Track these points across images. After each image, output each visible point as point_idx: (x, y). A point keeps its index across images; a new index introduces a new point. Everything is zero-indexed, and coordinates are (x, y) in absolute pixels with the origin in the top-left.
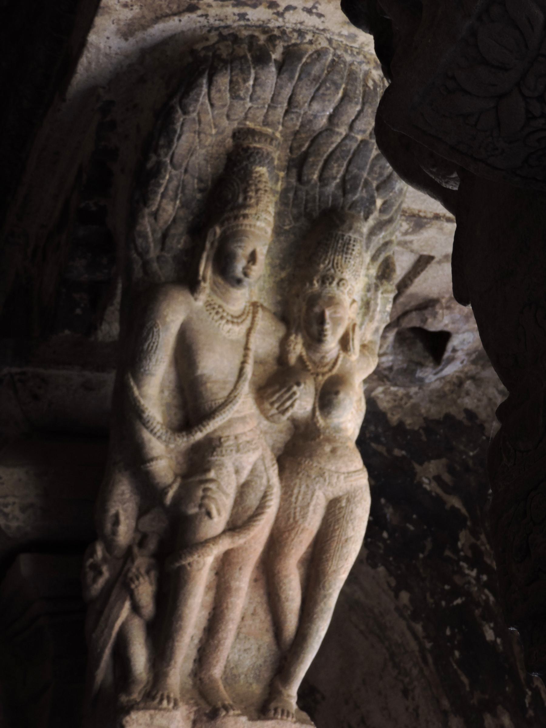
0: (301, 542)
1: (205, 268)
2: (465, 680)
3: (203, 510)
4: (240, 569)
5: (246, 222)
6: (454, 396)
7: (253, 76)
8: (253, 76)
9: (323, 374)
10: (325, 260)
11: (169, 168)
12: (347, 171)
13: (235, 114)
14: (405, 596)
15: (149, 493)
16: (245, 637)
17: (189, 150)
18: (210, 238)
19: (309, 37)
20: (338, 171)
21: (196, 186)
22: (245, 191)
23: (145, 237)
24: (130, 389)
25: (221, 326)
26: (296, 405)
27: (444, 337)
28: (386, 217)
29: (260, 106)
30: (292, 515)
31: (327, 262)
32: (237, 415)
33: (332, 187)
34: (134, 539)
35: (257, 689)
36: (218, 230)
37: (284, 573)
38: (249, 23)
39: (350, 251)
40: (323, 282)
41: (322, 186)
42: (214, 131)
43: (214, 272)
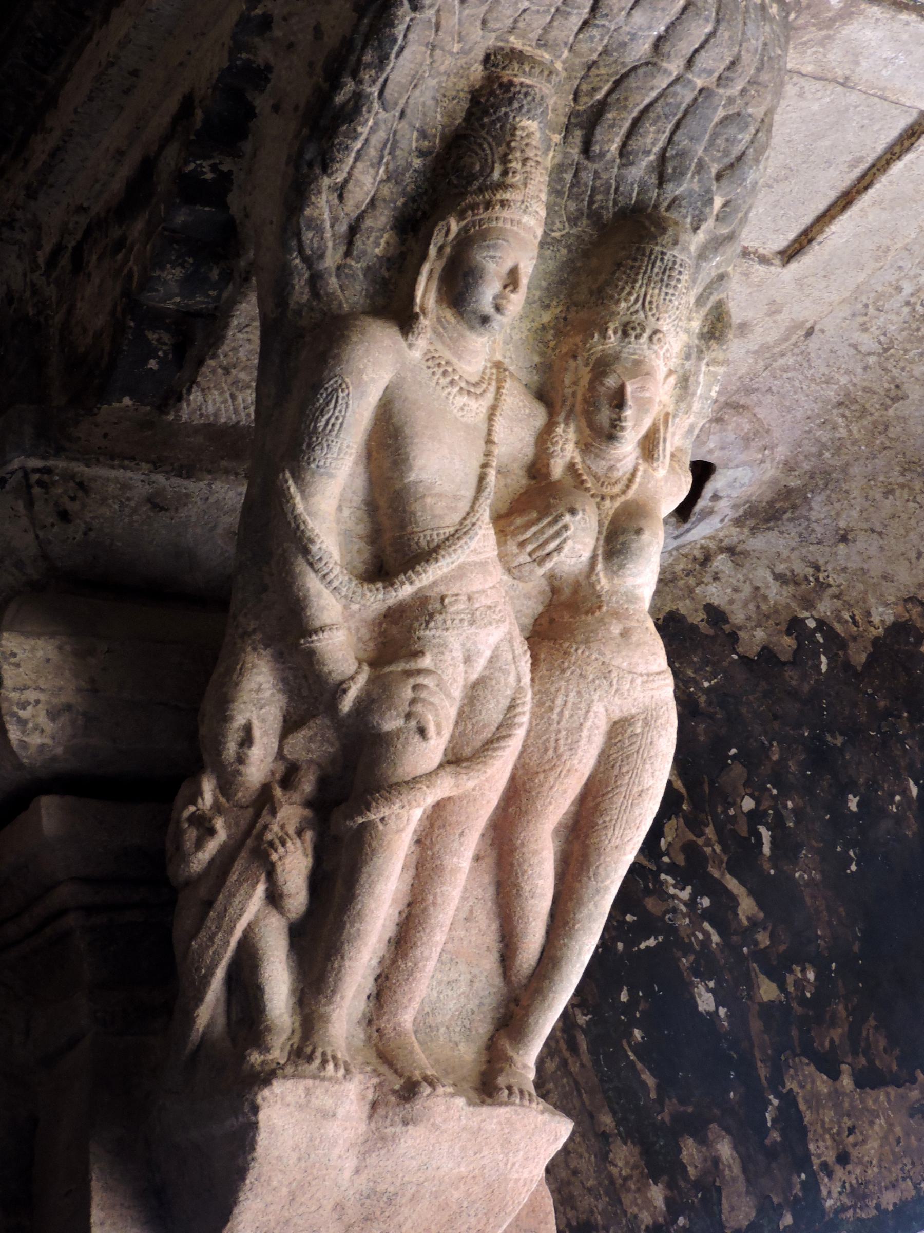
0: (565, 792)
1: (426, 291)
2: (649, 1079)
3: (413, 723)
4: (462, 834)
5: (506, 214)
6: (692, 581)
9: (613, 498)
10: (630, 294)
11: (376, 105)
12: (670, 140)
13: (497, 19)
16: (452, 960)
17: (413, 77)
18: (437, 239)
21: (414, 145)
22: (505, 160)
23: (320, 230)
24: (289, 498)
25: (451, 397)
28: (724, 230)
29: (542, 9)
30: (552, 744)
31: (633, 298)
33: (640, 170)
34: (273, 773)
35: (468, 1053)
36: (454, 227)
37: (533, 846)
39: (673, 283)
40: (625, 334)
41: (622, 166)
42: (456, 48)
43: (439, 301)
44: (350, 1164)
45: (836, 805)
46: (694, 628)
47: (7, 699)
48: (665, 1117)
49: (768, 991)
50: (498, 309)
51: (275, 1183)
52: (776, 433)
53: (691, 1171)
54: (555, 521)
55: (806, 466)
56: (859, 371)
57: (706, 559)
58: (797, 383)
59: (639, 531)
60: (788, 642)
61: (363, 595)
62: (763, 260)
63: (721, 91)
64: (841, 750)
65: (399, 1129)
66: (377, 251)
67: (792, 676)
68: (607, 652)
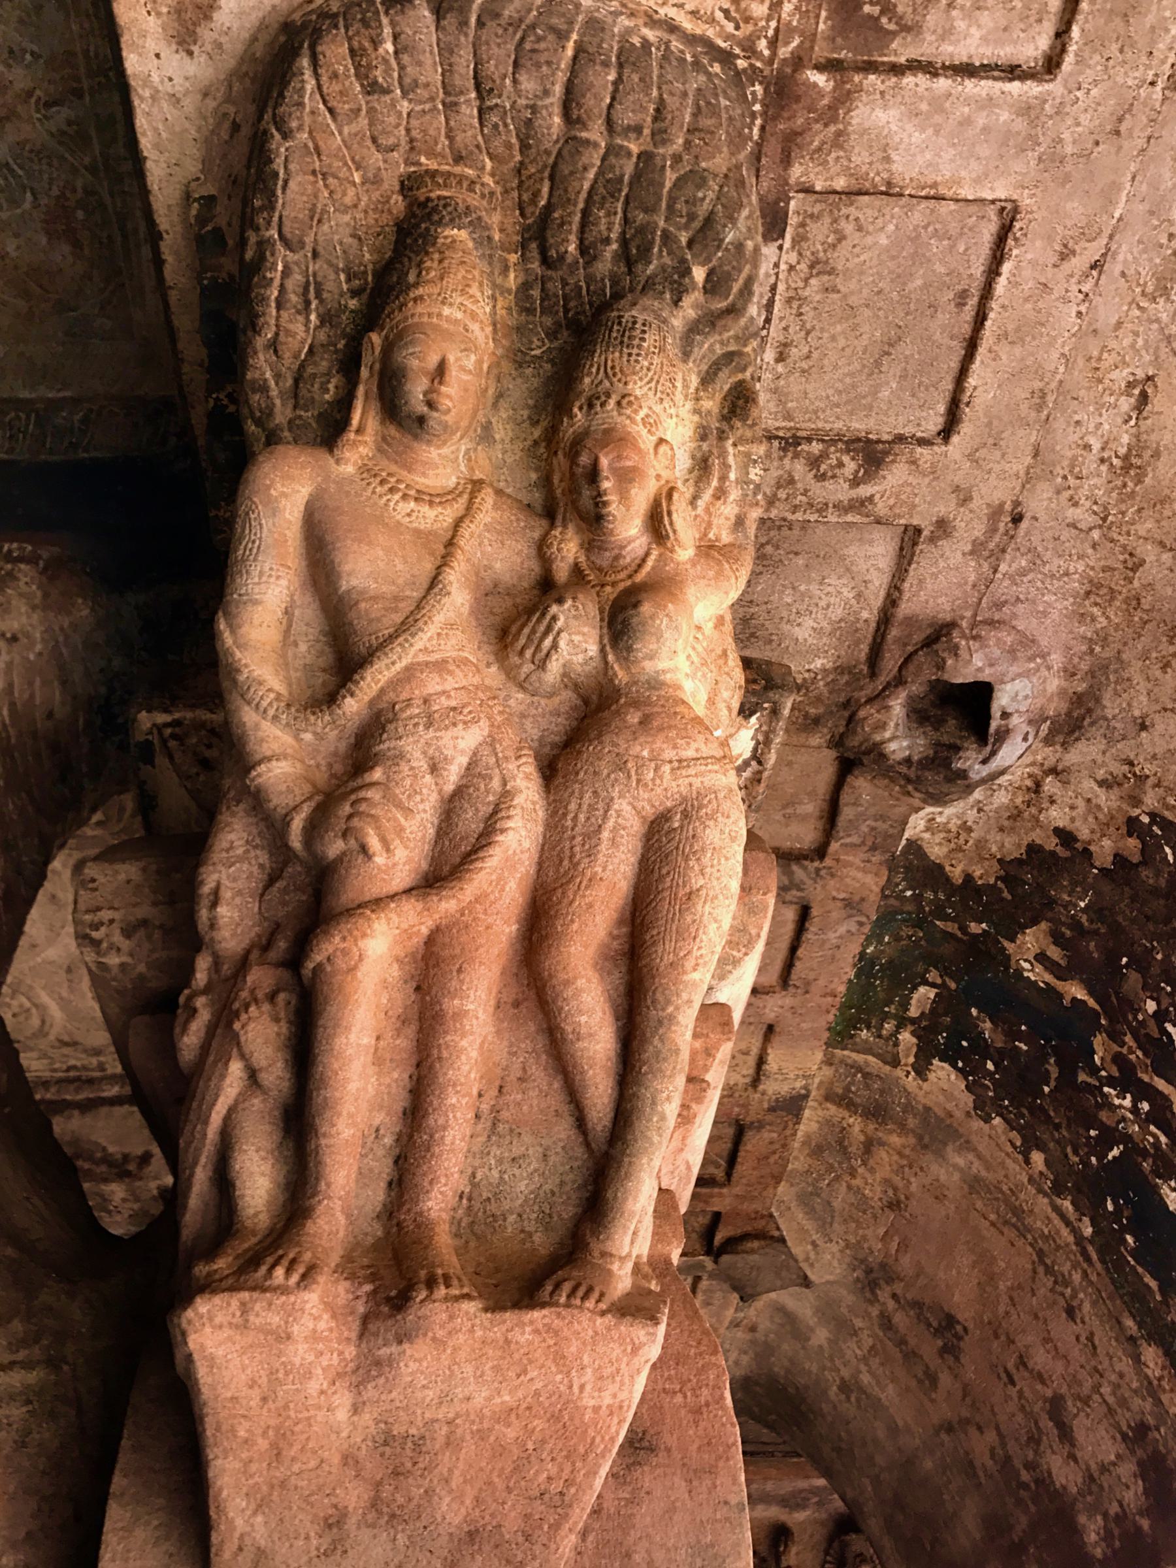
0: (590, 906)
4: (460, 971)
5: (420, 309)
6: (1033, 810)
7: (387, 31)
8: (387, 31)
10: (592, 366)
12: (626, 220)
13: (384, 132)
16: (511, 1130)
17: (313, 210)
18: (367, 359)
21: (345, 287)
25: (392, 504)
26: (562, 644)
27: (982, 693)
29: (427, 106)
30: (568, 853)
32: (422, 658)
37: (562, 976)
39: (636, 342)
40: (591, 406)
41: (588, 264)
42: (357, 177)
44: (343, 1400)
46: (1053, 854)
51: (242, 1433)
52: (1044, 642)
54: (543, 615)
55: (1084, 667)
56: (1090, 551)
57: (1038, 787)
58: (1039, 584)
59: (636, 605)
60: (1133, 843)
61: (307, 720)
62: (922, 442)
63: (661, 151)
65: (394, 1349)
66: (327, 397)
67: (1145, 873)
68: (621, 742)
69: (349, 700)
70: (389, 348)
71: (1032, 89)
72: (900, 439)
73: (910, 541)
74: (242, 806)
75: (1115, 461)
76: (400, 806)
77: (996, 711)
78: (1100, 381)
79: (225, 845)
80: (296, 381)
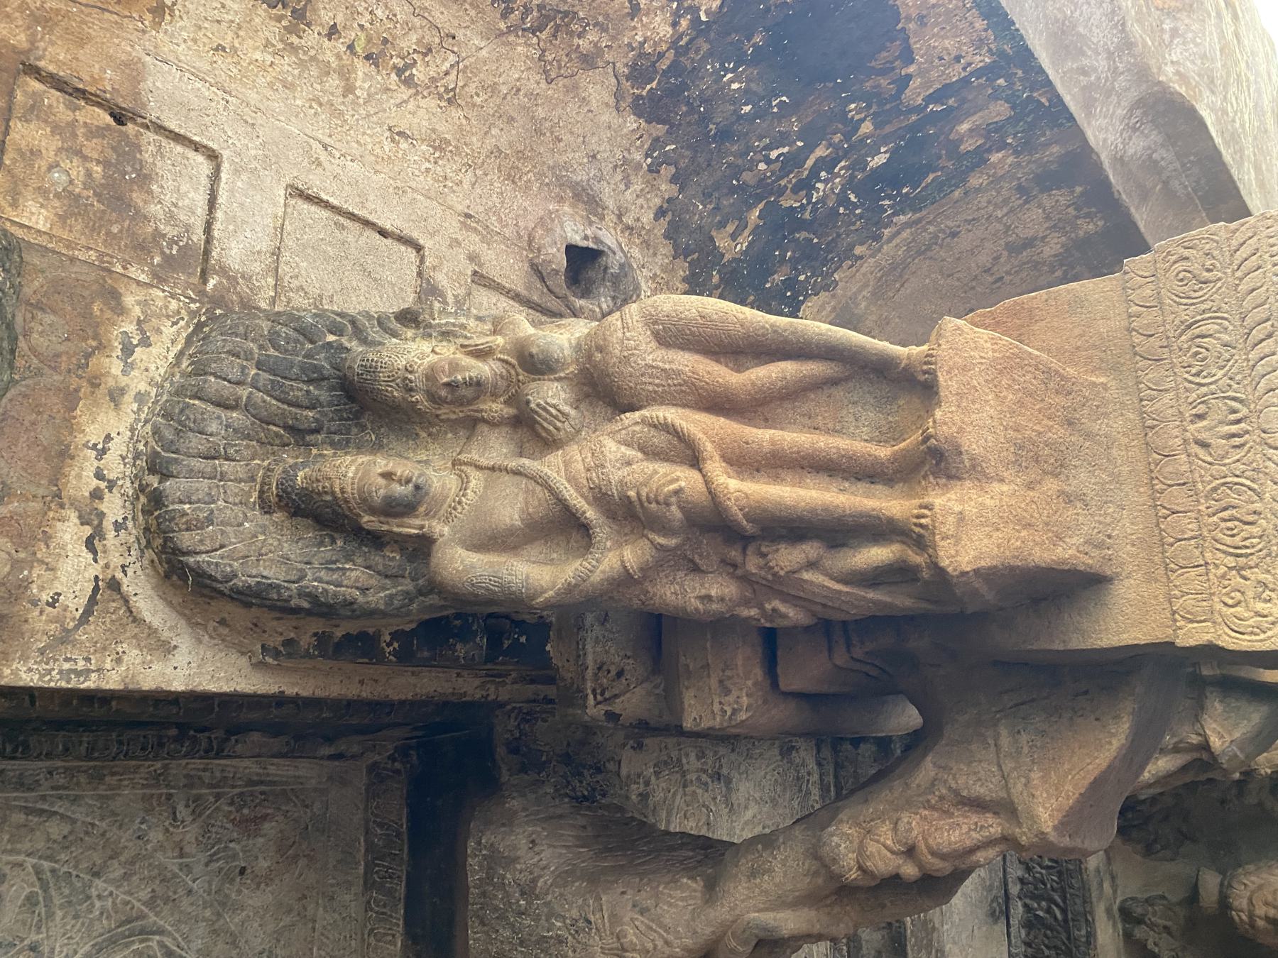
1: (410, 527)
2: (931, 177)
3: (673, 500)
4: (747, 443)
7: (177, 506)
8: (177, 506)
11: (304, 583)
14: (858, 250)
15: (667, 561)
19: (141, 447)
20: (299, 390)
22: (319, 494)
23: (391, 597)
27: (571, 250)
32: (563, 473)
36: (366, 518)
37: (749, 387)
38: (130, 517)
40: (411, 390)
42: (261, 537)
45: (750, 118)
47: (721, 723)
48: (950, 164)
49: (867, 127)
50: (408, 481)
52: (541, 213)
53: (980, 142)
54: (536, 413)
57: (628, 228)
59: (531, 356)
62: (422, 261)
64: (717, 124)
69: (588, 515)
70: (373, 511)
71: (225, 167)
72: (420, 274)
73: (480, 279)
74: (650, 589)
75: (437, 155)
76: (651, 477)
77: (584, 244)
78: (390, 158)
79: (673, 597)
80: (386, 576)
